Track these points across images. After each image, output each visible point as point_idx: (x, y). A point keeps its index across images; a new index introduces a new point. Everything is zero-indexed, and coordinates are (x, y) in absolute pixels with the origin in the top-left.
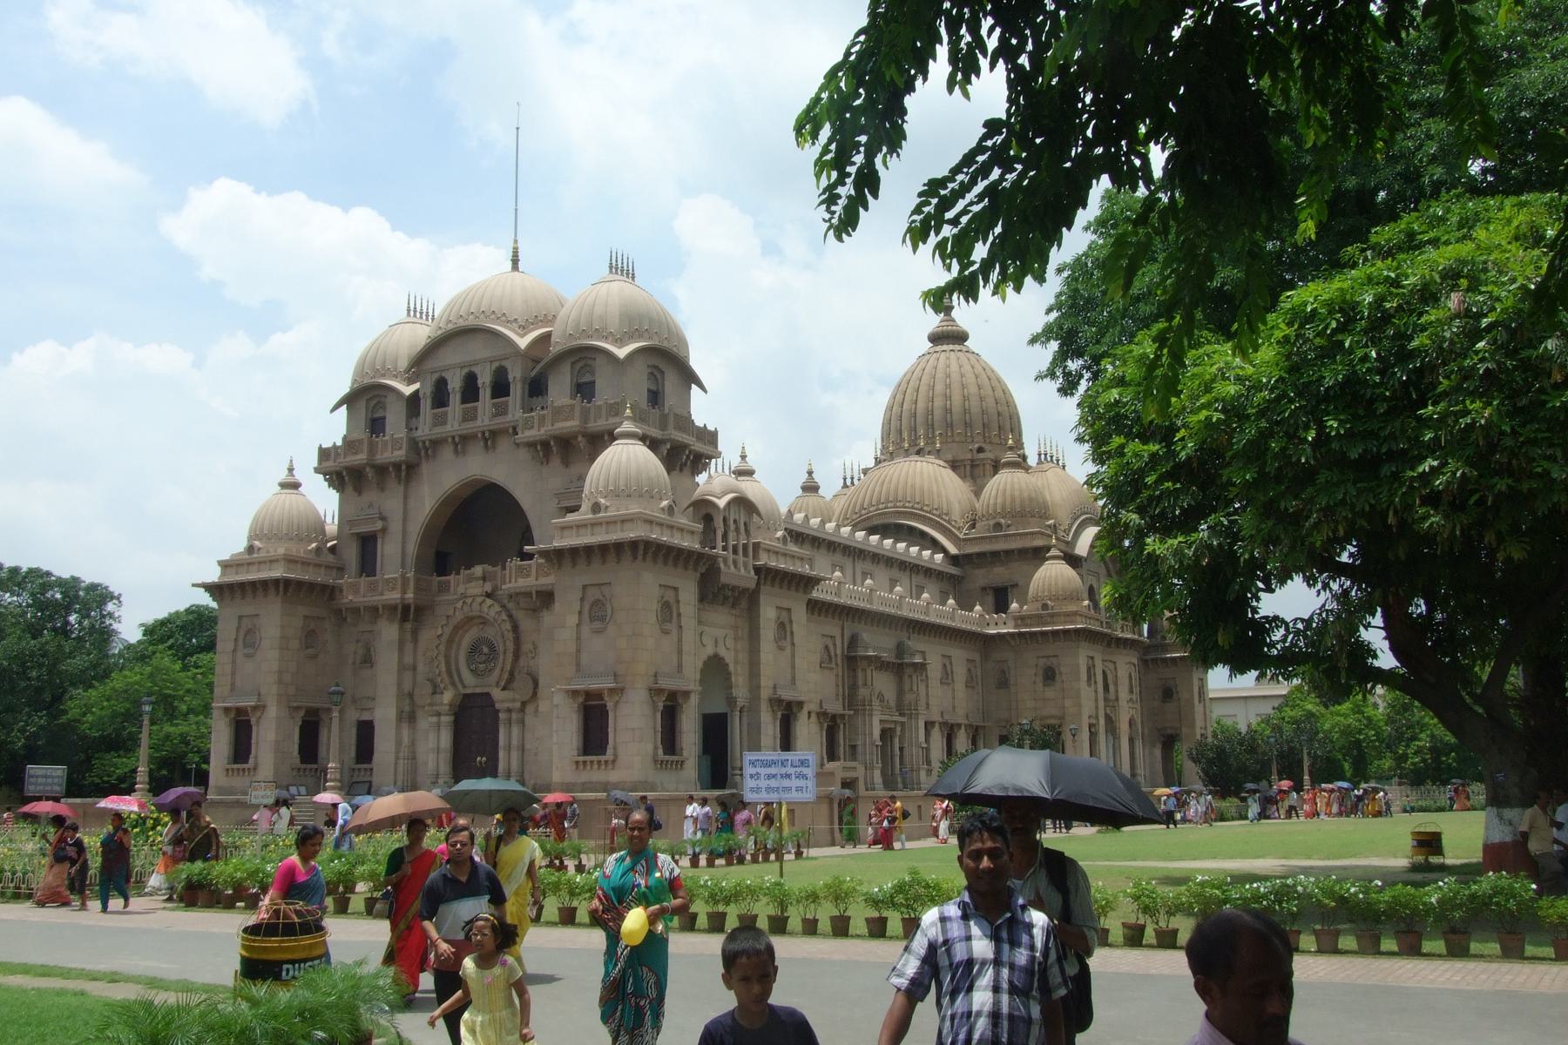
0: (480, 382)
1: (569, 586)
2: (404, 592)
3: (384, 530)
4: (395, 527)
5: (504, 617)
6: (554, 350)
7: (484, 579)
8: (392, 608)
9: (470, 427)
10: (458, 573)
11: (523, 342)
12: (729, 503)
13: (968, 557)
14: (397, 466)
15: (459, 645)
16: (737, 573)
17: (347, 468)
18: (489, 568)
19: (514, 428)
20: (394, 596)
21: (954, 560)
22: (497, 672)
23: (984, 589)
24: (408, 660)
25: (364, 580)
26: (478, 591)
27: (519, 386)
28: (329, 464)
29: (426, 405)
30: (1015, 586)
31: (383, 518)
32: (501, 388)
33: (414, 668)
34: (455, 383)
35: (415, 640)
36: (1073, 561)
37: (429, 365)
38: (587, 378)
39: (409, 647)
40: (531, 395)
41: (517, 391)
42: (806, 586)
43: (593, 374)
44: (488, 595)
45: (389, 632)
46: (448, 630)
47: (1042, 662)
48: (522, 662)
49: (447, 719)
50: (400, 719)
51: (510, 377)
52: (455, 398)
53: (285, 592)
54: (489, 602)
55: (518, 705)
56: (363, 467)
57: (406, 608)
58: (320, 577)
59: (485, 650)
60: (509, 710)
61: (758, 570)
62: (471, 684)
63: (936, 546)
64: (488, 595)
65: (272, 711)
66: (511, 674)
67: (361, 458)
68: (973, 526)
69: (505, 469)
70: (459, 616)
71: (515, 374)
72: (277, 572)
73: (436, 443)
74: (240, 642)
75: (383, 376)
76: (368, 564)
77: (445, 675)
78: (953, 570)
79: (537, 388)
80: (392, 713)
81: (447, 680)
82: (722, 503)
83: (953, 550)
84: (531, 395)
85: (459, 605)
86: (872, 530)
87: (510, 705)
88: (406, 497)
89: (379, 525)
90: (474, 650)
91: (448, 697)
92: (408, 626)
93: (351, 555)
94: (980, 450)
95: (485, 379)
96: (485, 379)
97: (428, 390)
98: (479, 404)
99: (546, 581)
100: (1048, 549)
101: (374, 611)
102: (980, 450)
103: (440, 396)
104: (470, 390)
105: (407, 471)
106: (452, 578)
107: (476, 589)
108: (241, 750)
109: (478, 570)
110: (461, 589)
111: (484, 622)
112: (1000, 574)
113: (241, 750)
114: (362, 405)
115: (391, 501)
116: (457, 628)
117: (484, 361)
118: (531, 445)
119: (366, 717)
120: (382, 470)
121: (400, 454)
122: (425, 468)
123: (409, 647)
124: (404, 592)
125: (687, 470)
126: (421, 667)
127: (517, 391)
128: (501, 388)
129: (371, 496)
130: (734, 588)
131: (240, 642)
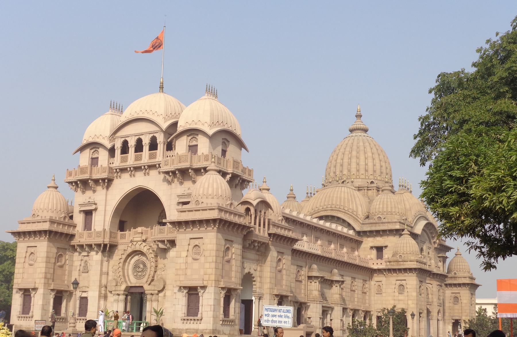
0: (143, 143)
1: (183, 238)
2: (104, 238)
3: (96, 209)
4: (101, 208)
5: (151, 251)
6: (180, 129)
7: (142, 233)
8: (99, 245)
9: (138, 163)
10: (130, 231)
11: (165, 126)
12: (258, 203)
13: (365, 233)
14: (103, 180)
15: (129, 263)
16: (261, 233)
17: (80, 180)
18: (144, 228)
19: (159, 165)
20: (99, 241)
21: (359, 233)
22: (147, 276)
23: (372, 248)
24: (105, 270)
25: (86, 232)
26: (139, 239)
27: (162, 145)
28: (72, 179)
29: (118, 152)
30: (386, 247)
31: (96, 204)
32: (153, 146)
33: (108, 274)
34: (132, 143)
35: (108, 261)
36: (414, 236)
37: (119, 134)
38: (194, 143)
39: (105, 264)
40: (167, 150)
41: (161, 147)
42: (291, 242)
43: (197, 141)
44: (144, 241)
45: (96, 257)
46: (124, 257)
47: (398, 283)
48: (158, 272)
49: (122, 297)
50: (100, 297)
51: (158, 141)
52: (132, 150)
53: (49, 236)
54: (144, 244)
55: (156, 292)
56: (88, 180)
57: (105, 245)
58: (65, 230)
59: (141, 266)
60: (152, 294)
61: (270, 235)
62: (133, 281)
63: (349, 226)
64: (144, 241)
65: (41, 291)
66: (153, 277)
67: (86, 176)
68: (368, 217)
70: (130, 250)
71: (160, 138)
72: (46, 226)
73: (123, 170)
75: (98, 138)
76: (88, 226)
77: (122, 277)
78: (357, 238)
79: (170, 147)
80: (97, 294)
81: (123, 280)
82: (255, 203)
83: (358, 229)
84: (167, 150)
85: (130, 245)
86: (321, 218)
87: (153, 292)
88: (106, 195)
89: (93, 207)
90: (136, 266)
91: (123, 287)
93: (79, 219)
94: (372, 182)
95: (146, 141)
96: (146, 141)
97: (118, 145)
98: (143, 153)
99: (170, 237)
100: (403, 230)
101: (90, 246)
102: (372, 182)
103: (125, 149)
104: (139, 147)
105: (108, 182)
106: (127, 233)
108: (26, 308)
109: (139, 229)
111: (141, 253)
112: (379, 241)
113: (26, 308)
116: (129, 255)
118: (167, 173)
119: (84, 295)
120: (96, 181)
121: (105, 175)
122: (116, 182)
123: (105, 264)
124: (104, 238)
125: (239, 187)
126: (110, 273)
127: (161, 147)
128: (153, 146)
129: (89, 193)
130: (259, 242)
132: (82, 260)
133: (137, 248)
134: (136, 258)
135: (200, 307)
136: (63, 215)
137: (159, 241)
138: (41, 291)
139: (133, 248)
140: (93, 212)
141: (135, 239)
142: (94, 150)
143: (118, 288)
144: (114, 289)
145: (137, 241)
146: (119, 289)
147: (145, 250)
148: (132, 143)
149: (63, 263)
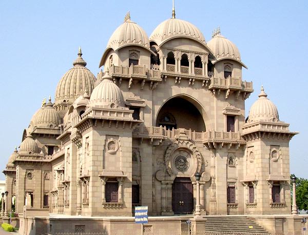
14: (154, 82)
26: (186, 139)
37: (167, 46)
54: (190, 143)
59: (183, 161)
69: (197, 95)
71: (204, 60)
74: (107, 147)
91: (173, 178)
92: (154, 147)
95: (191, 58)
96: (191, 58)
107: (184, 137)
114: (126, 54)
117: (193, 52)
118: (217, 90)
120: (148, 82)
131: (107, 147)
133: (184, 145)
134: (178, 153)
135: (255, 196)
136: (272, 118)
137: (215, 142)
138: (260, 183)
140: (141, 108)
141: (181, 138)
142: (133, 52)
143: (169, 178)
146: (168, 179)
147: (191, 148)
148: (178, 56)
149: (277, 158)
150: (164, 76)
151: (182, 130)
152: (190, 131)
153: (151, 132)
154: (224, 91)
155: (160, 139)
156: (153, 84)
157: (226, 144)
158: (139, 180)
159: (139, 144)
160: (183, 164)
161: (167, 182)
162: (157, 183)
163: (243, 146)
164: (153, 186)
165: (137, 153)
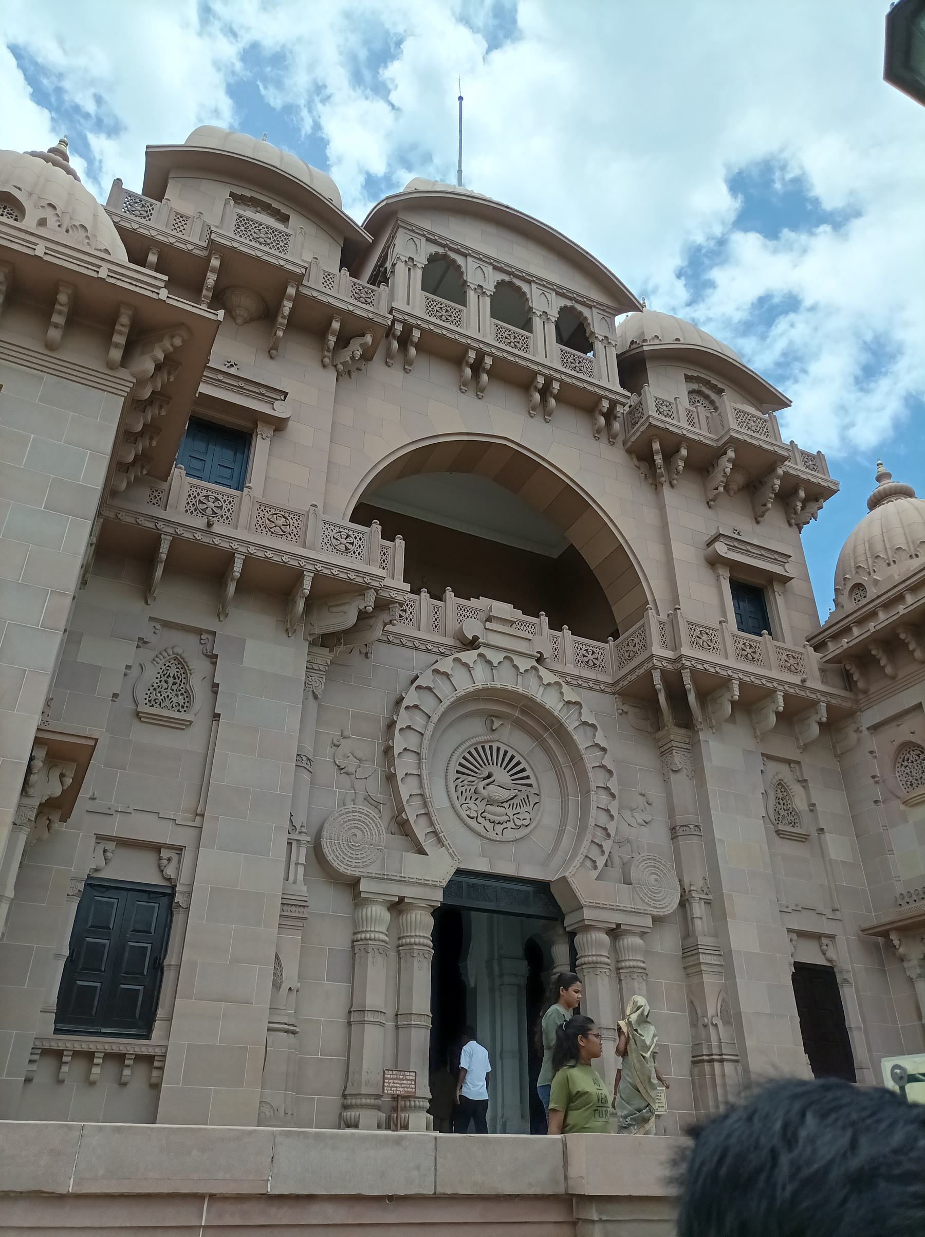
8: (330, 590)
26: (522, 647)
37: (426, 223)
45: (264, 656)
49: (421, 926)
59: (502, 775)
60: (615, 932)
92: (324, 656)
95: (545, 305)
96: (545, 305)
110: (472, 628)
115: (301, 385)
119: (140, 871)
132: (142, 642)
134: (474, 730)
139: (481, 678)
144: (374, 870)
145: (509, 655)
147: (551, 701)
150: (408, 327)
151: (503, 609)
152: (544, 619)
153: (315, 531)
154: (703, 463)
155: (360, 590)
156: (344, 341)
157: (751, 701)
158: (179, 850)
159: (221, 613)
160: (505, 794)
161: (397, 890)
162: (326, 902)
163: (835, 724)
164: (292, 913)
165: (198, 666)
